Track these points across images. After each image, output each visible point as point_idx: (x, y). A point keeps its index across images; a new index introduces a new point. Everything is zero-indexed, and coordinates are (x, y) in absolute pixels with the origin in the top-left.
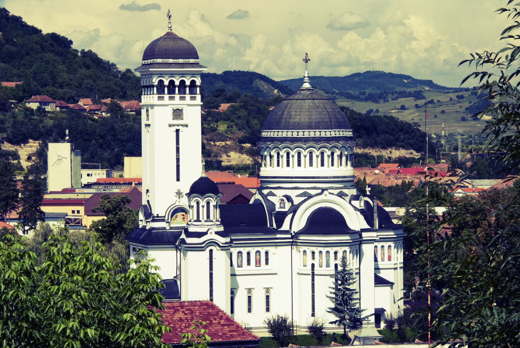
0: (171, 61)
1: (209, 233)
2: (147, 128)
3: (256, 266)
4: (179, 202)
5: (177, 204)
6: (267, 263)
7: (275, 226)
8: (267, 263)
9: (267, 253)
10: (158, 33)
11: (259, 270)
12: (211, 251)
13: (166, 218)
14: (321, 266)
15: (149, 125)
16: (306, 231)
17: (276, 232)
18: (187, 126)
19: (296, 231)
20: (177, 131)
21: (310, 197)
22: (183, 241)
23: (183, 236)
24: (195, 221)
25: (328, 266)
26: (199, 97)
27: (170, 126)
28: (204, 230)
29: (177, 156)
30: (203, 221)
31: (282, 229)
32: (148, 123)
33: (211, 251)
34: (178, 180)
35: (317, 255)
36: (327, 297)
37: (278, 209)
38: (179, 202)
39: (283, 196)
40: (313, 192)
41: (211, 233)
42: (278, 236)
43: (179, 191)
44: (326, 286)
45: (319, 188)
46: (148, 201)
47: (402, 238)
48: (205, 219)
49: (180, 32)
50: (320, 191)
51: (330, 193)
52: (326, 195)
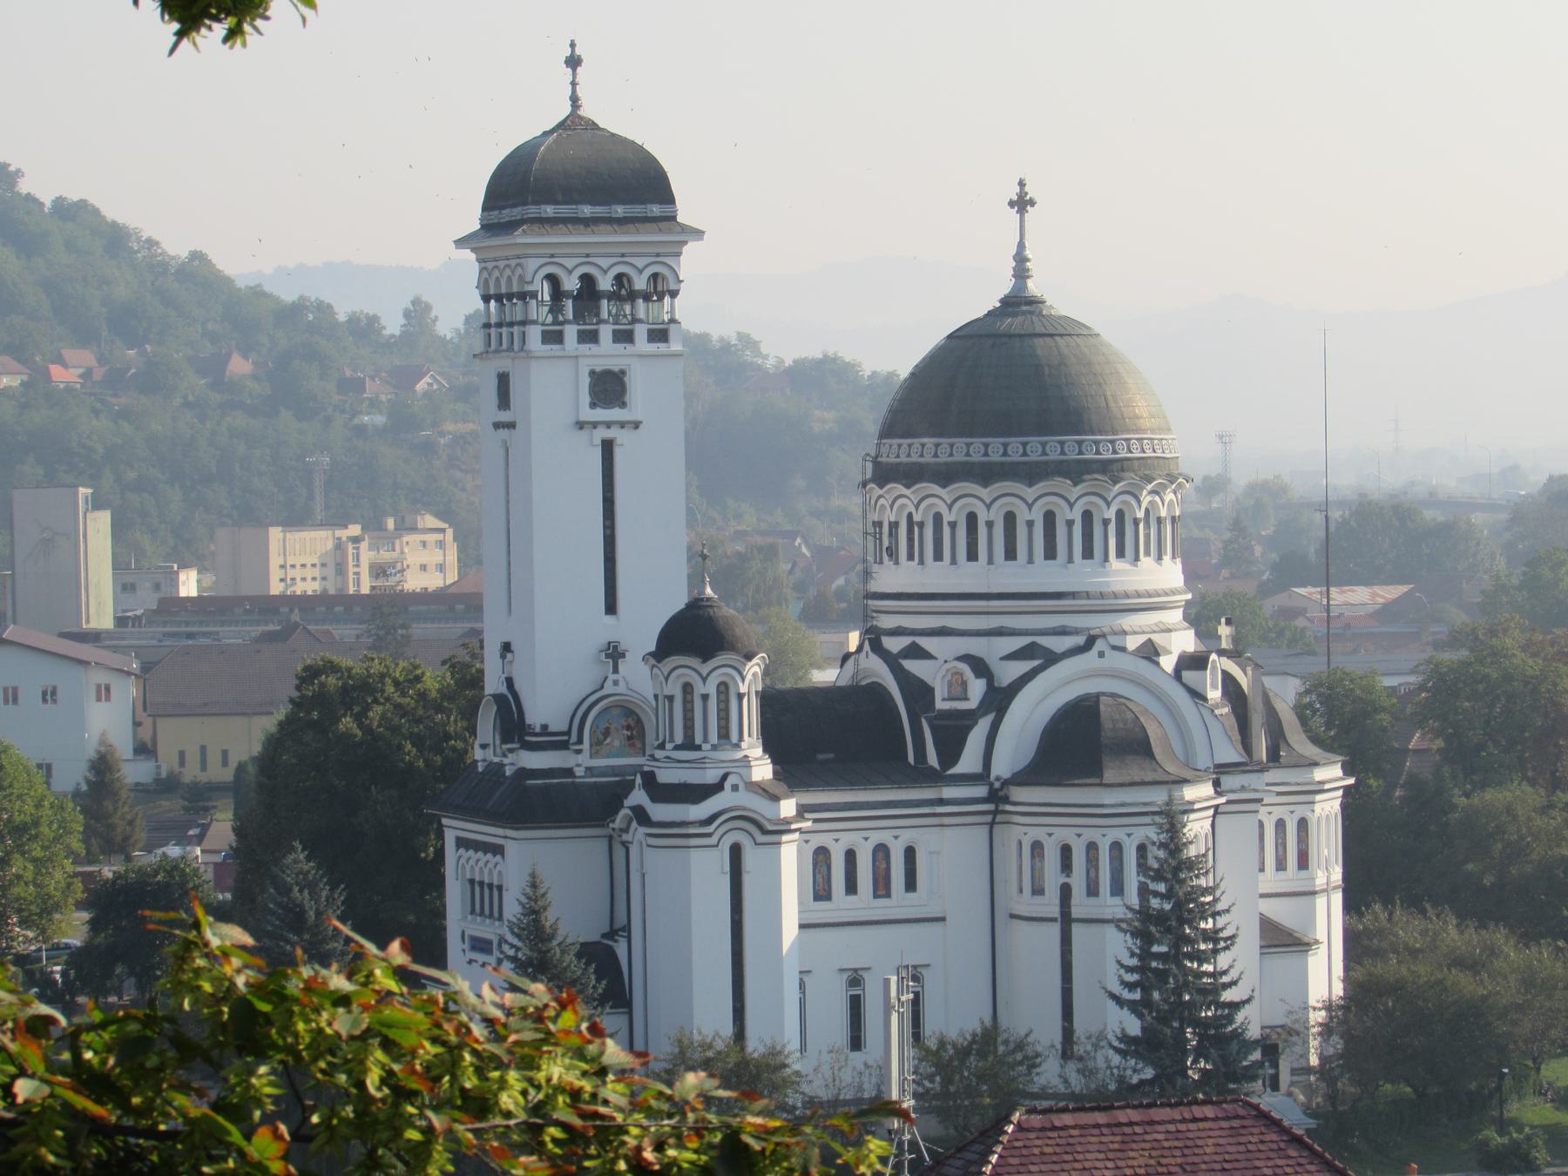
0: (587, 210)
1: (727, 785)
2: (504, 433)
3: (876, 896)
4: (616, 683)
5: (609, 688)
6: (911, 885)
7: (933, 759)
8: (911, 885)
9: (910, 853)
10: (530, 117)
11: (882, 909)
12: (736, 852)
13: (574, 738)
14: (1092, 891)
15: (511, 426)
16: (1033, 774)
17: (923, 775)
19: (1006, 774)
20: (608, 447)
21: (1051, 658)
22: (641, 816)
23: (638, 797)
24: (677, 748)
25: (1118, 889)
27: (581, 425)
28: (711, 776)
29: (605, 527)
30: (705, 746)
31: (959, 769)
32: (504, 416)
33: (736, 852)
34: (611, 608)
36: (1113, 996)
37: (940, 705)
38: (616, 683)
39: (959, 659)
41: (735, 788)
42: (949, 792)
43: (615, 648)
44: (1108, 953)
45: (1075, 632)
46: (510, 682)
47: (1340, 793)
48: (714, 737)
49: (611, 113)
50: (1080, 640)
51: (1114, 648)
52: (1101, 654)
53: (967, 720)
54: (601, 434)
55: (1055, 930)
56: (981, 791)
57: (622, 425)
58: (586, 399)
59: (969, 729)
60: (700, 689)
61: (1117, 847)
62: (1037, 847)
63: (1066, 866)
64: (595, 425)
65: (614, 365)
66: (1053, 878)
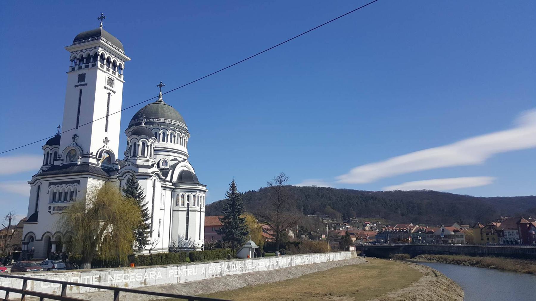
12: (154, 181)
21: (180, 162)
26: (122, 76)
27: (105, 88)
33: (154, 181)
34: (106, 131)
35: (192, 198)
40: (180, 159)
53: (168, 170)
54: (109, 91)
55: (186, 212)
56: (171, 184)
58: (107, 83)
59: (169, 172)
62: (183, 195)
66: (186, 202)
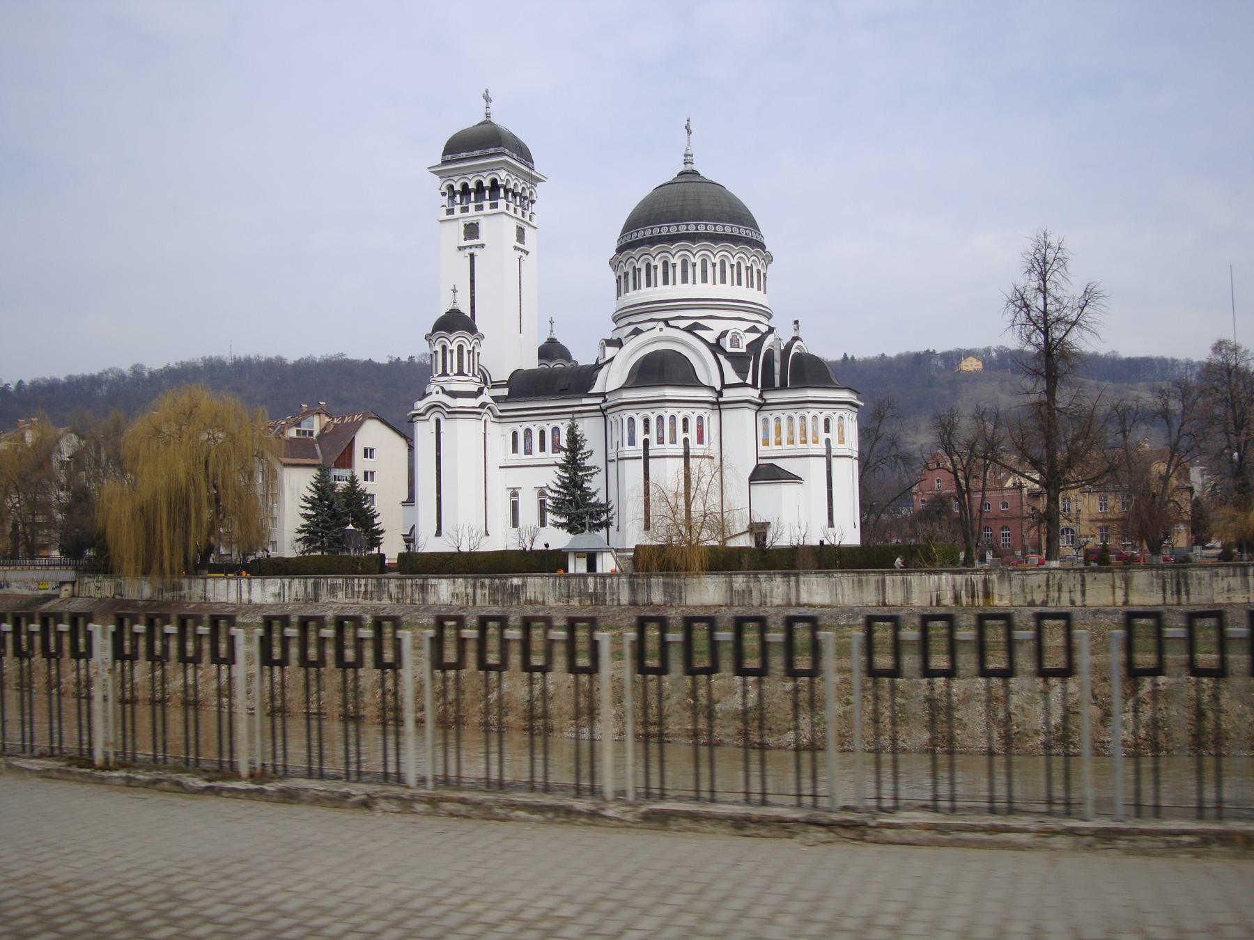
0: (464, 155)
18: (482, 246)
20: (472, 256)
48: (455, 371)
54: (468, 251)
55: (641, 462)
57: (476, 246)
60: (450, 347)
61: (673, 418)
63: (647, 430)
64: (465, 248)
65: (473, 220)
